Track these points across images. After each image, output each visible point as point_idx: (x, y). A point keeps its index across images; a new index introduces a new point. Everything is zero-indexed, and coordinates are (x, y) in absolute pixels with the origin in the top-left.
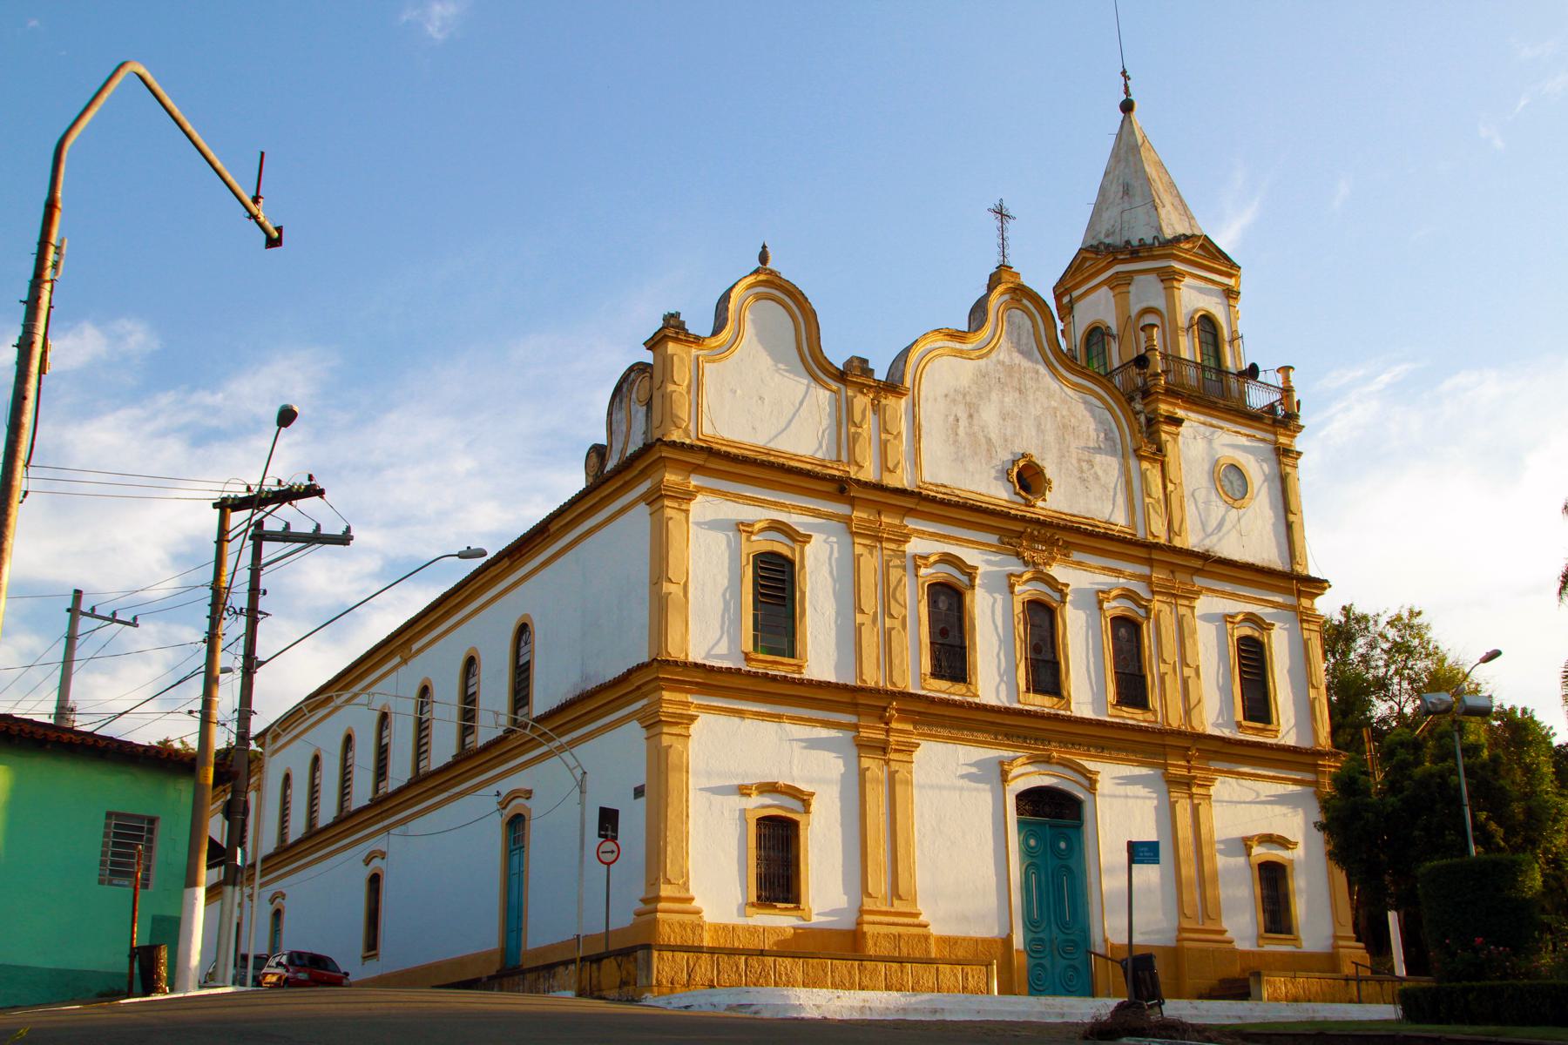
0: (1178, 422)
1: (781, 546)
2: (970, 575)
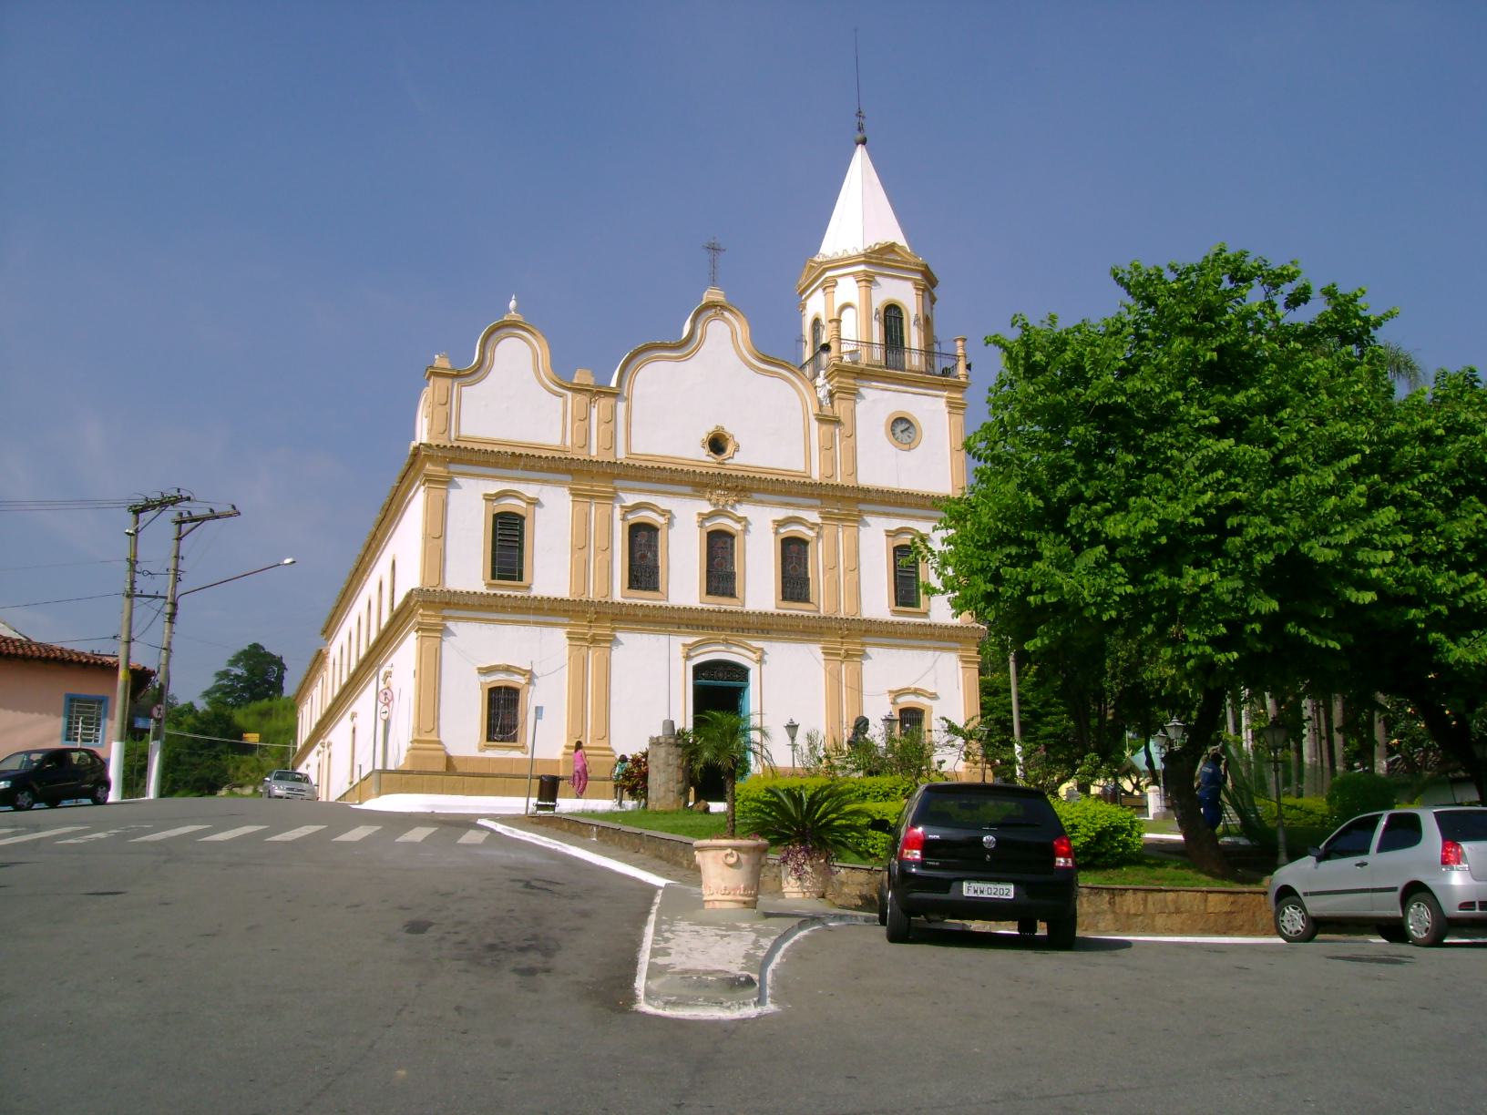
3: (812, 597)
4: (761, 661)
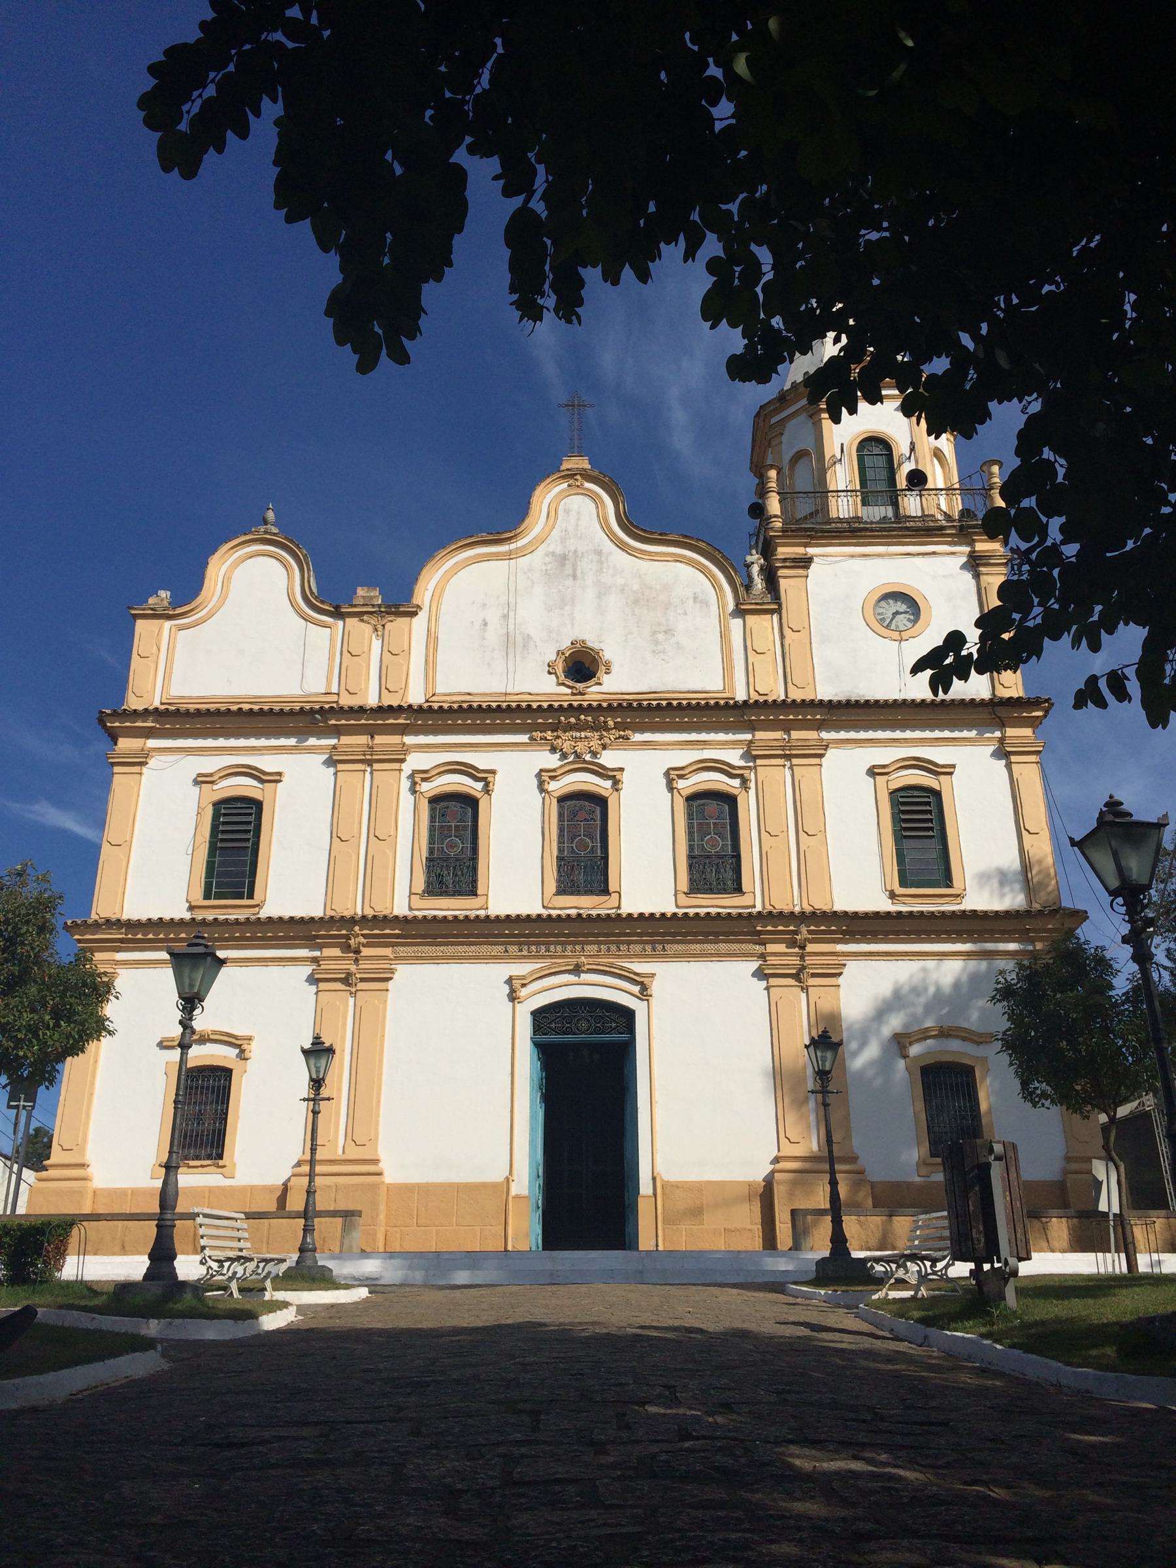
0: (805, 563)
1: (244, 786)
2: (484, 779)
3: (745, 886)
4: (644, 993)
